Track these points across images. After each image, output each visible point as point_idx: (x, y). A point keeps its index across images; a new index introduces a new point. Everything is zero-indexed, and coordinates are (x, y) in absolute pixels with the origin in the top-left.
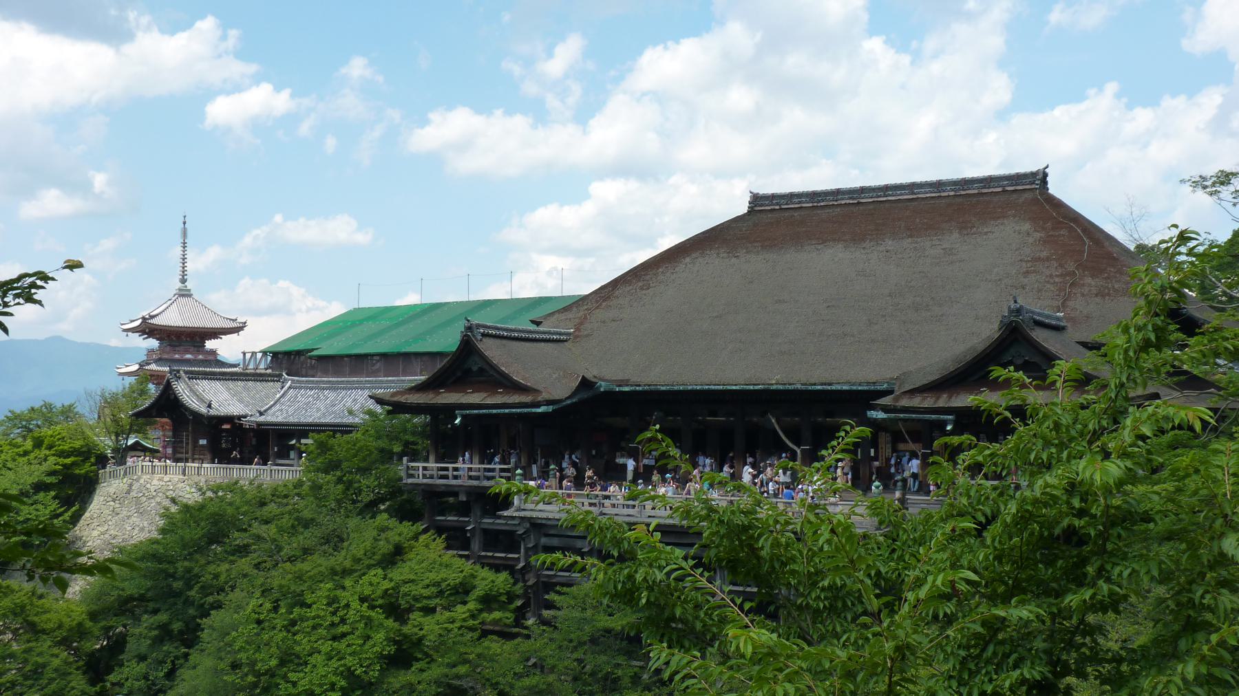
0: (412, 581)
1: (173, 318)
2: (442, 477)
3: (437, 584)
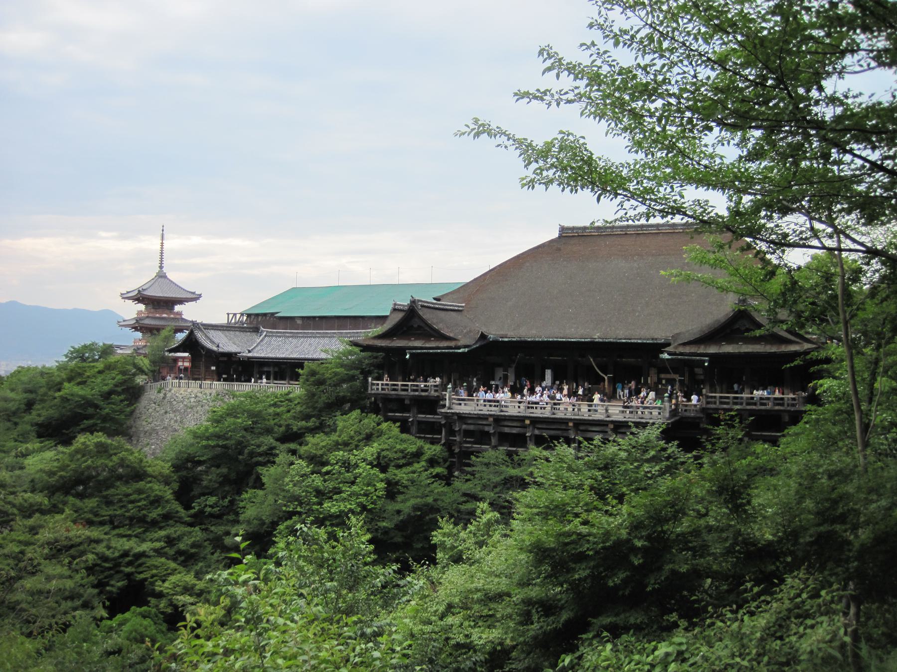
2: (394, 390)
3: (402, 451)
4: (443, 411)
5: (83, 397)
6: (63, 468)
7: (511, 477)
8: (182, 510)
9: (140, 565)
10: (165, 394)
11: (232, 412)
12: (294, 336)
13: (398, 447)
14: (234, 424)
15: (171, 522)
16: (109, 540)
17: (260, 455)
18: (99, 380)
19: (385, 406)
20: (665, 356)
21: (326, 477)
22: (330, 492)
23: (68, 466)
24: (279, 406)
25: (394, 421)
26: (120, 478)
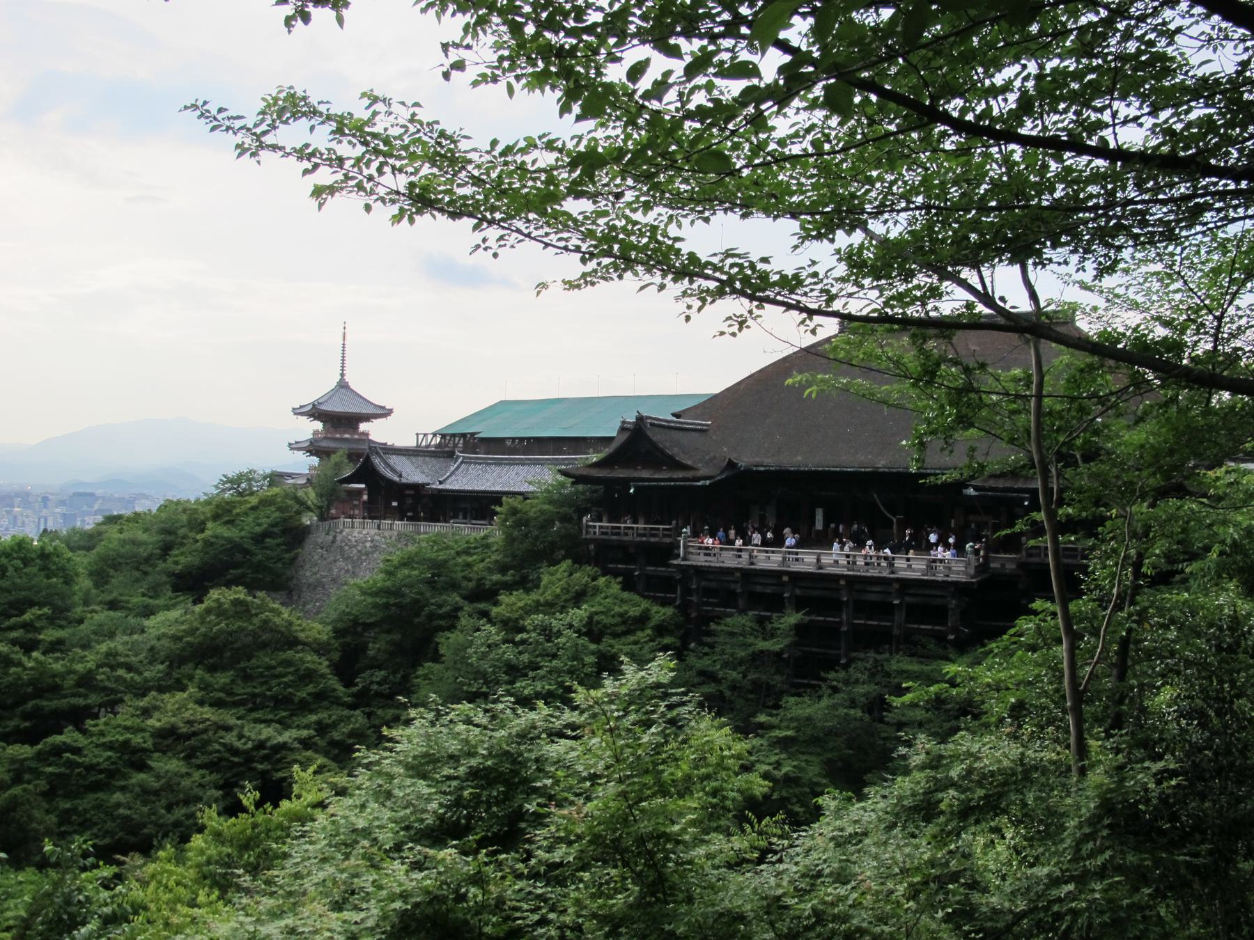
3: (621, 615)
4: (675, 562)
5: (229, 540)
6: (192, 632)
7: (762, 652)
8: (342, 689)
9: (279, 761)
10: (335, 537)
11: (407, 563)
12: (499, 463)
13: (617, 609)
14: (410, 576)
15: (325, 703)
16: (242, 727)
17: (442, 617)
18: (250, 519)
19: (606, 556)
20: (971, 491)
21: (521, 648)
22: (525, 667)
23: (198, 629)
24: (471, 555)
25: (615, 574)
26: (264, 645)
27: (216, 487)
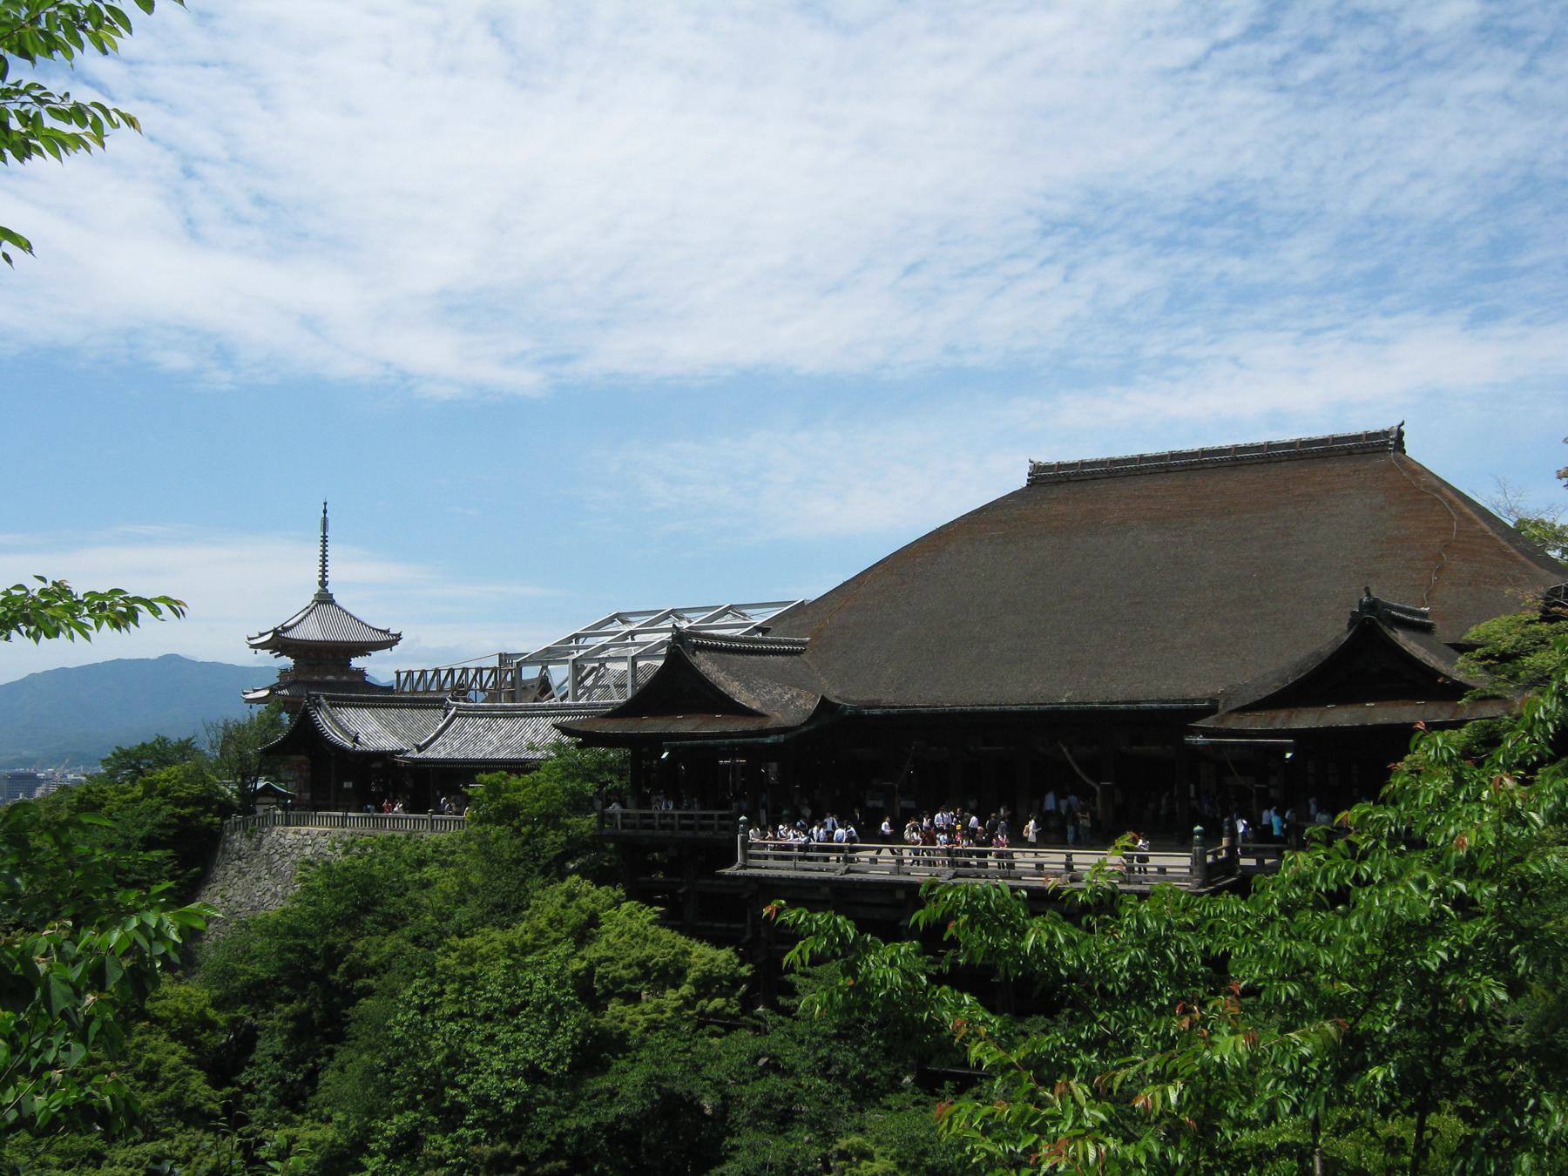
0: (611, 959)
1: (310, 631)
3: (642, 964)
13: (635, 953)
27: (105, 762)
